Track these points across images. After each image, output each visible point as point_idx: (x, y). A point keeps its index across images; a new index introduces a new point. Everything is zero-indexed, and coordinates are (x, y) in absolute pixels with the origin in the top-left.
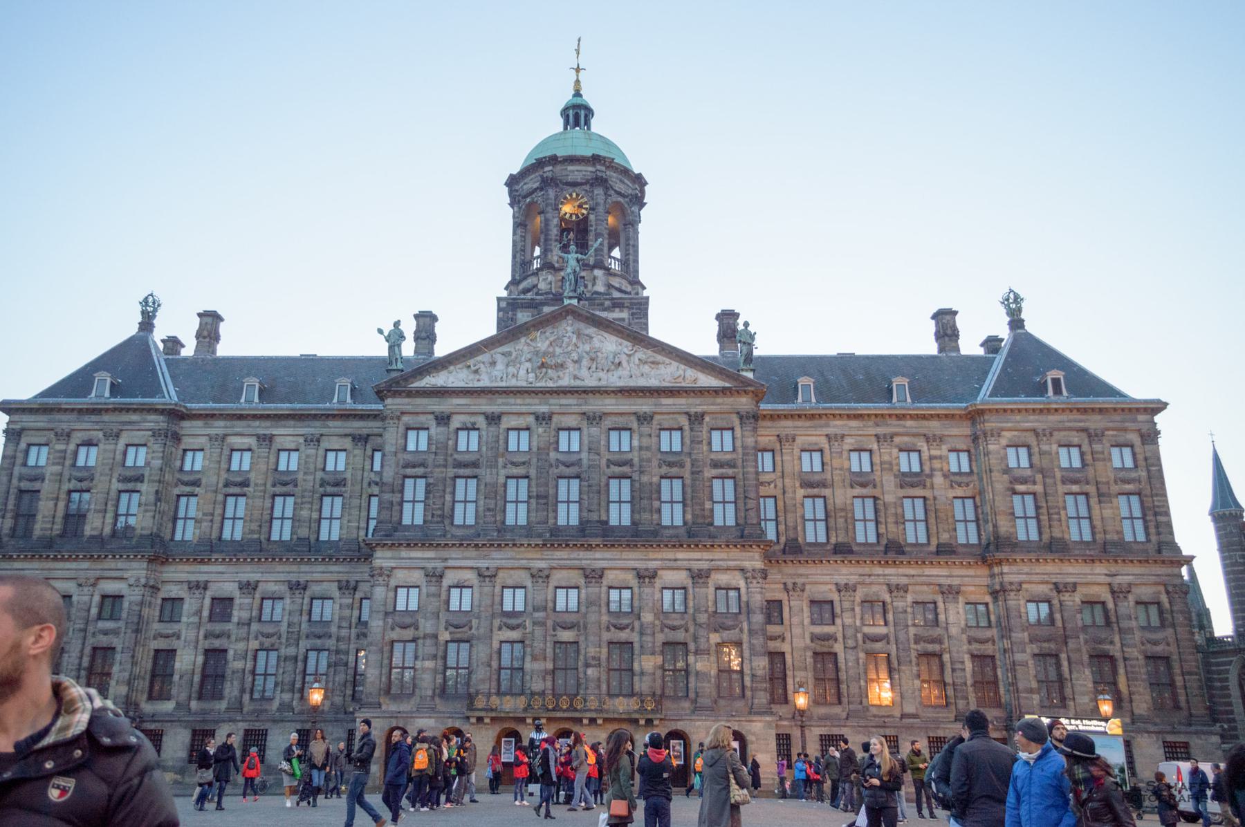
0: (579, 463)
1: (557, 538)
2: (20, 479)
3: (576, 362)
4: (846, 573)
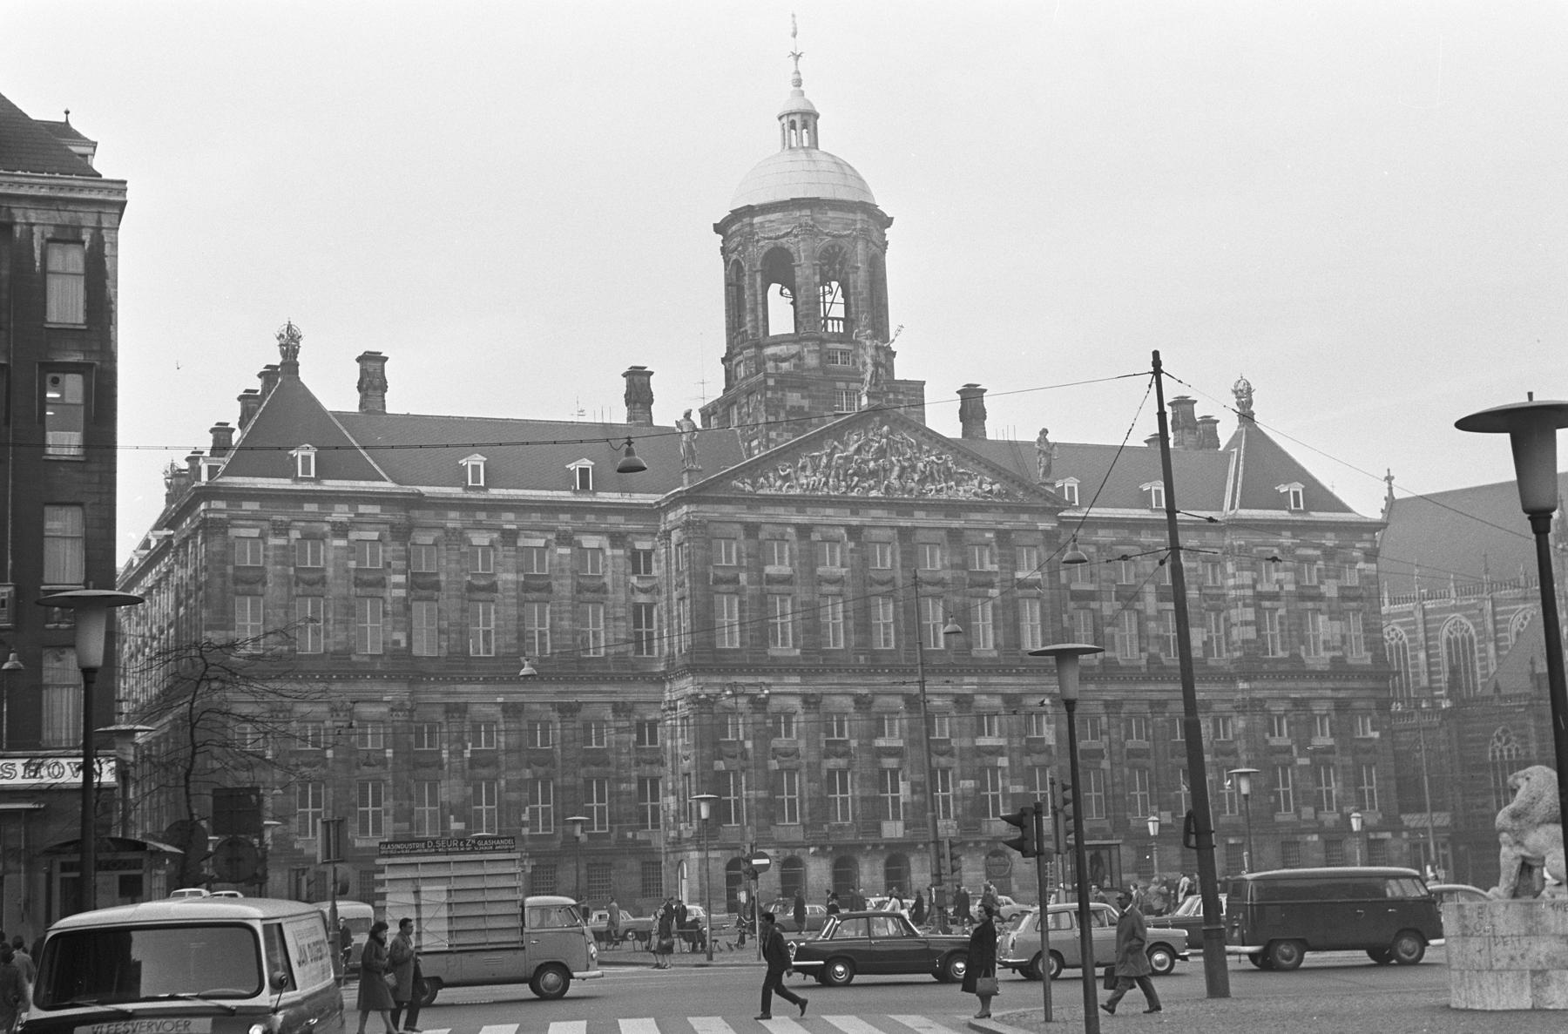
0: (892, 581)
1: (876, 664)
2: (237, 581)
3: (885, 470)
4: (1113, 691)
